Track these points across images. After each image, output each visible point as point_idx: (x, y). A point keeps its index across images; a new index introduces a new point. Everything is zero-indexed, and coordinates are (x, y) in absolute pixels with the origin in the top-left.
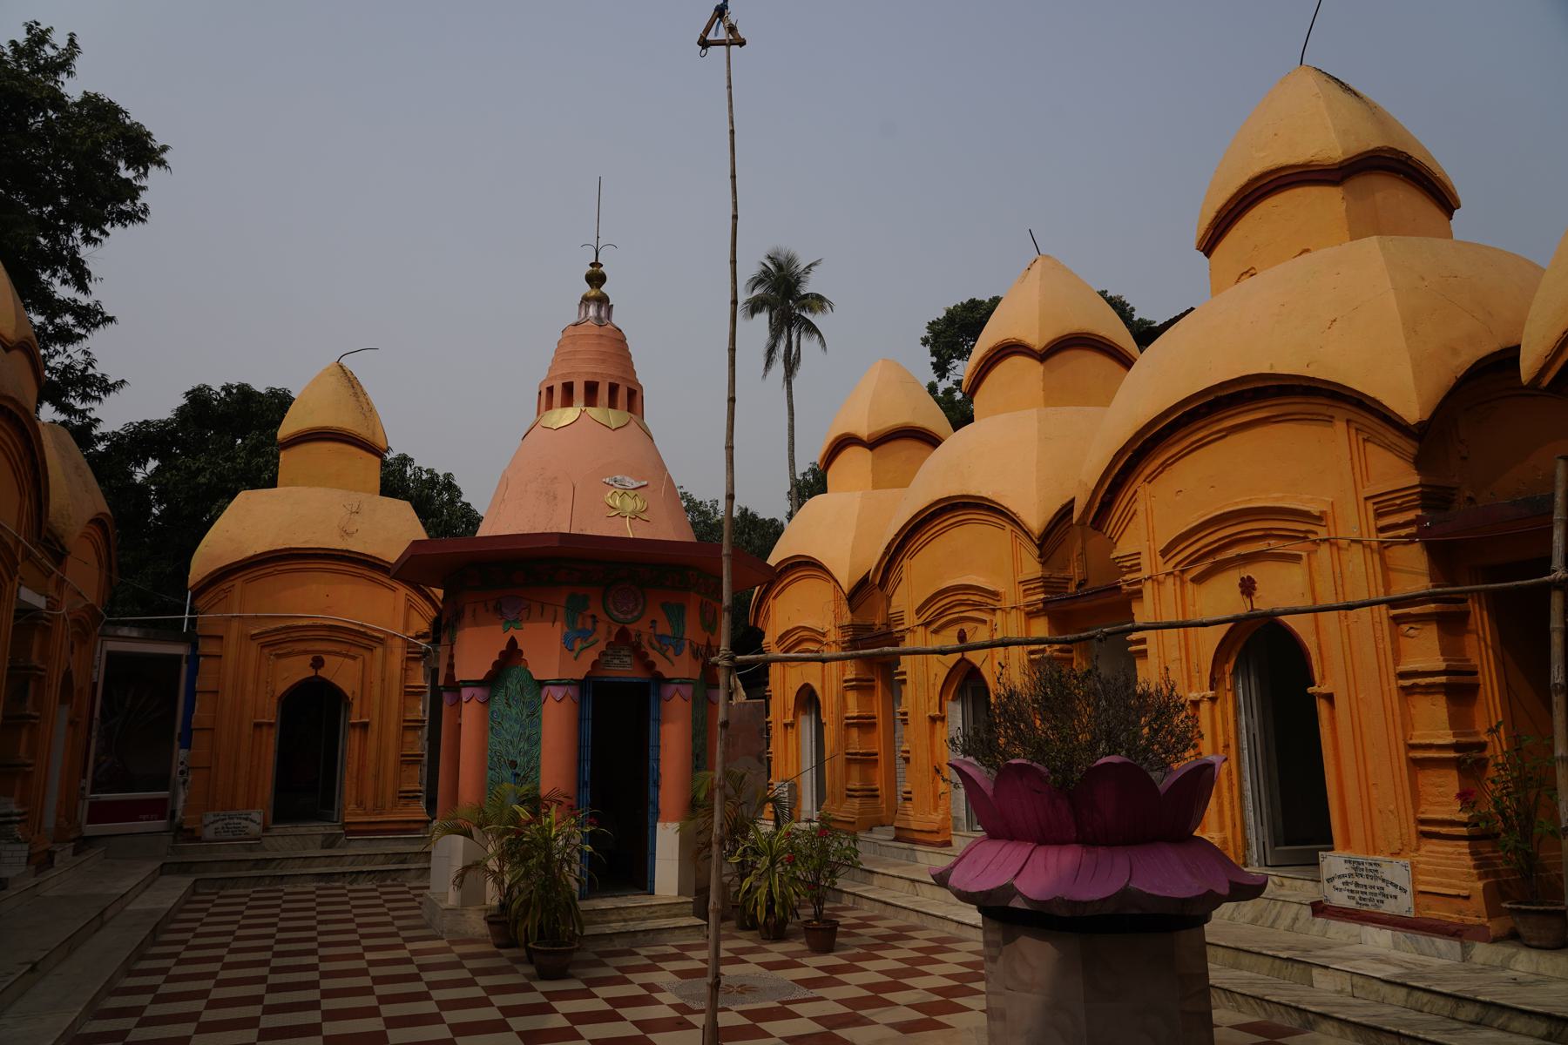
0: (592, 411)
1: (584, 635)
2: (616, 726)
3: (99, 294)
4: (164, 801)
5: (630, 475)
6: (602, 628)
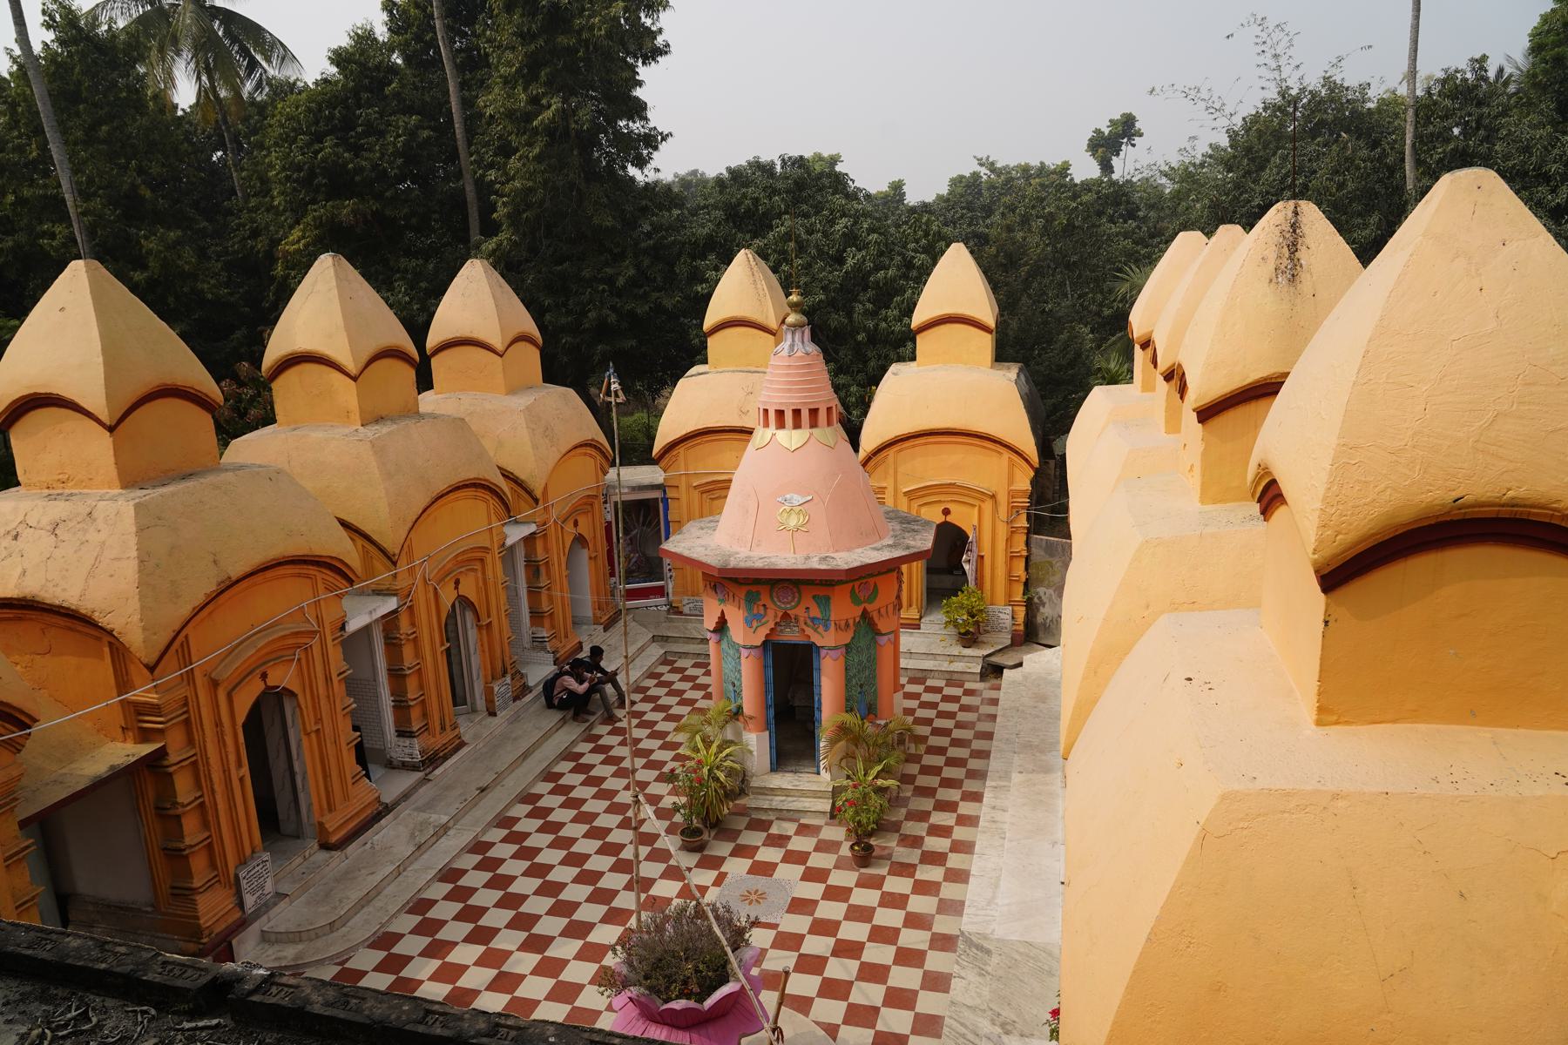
0: (781, 434)
1: (759, 617)
2: (790, 670)
3: (657, 119)
4: (662, 587)
5: (798, 493)
6: (771, 613)
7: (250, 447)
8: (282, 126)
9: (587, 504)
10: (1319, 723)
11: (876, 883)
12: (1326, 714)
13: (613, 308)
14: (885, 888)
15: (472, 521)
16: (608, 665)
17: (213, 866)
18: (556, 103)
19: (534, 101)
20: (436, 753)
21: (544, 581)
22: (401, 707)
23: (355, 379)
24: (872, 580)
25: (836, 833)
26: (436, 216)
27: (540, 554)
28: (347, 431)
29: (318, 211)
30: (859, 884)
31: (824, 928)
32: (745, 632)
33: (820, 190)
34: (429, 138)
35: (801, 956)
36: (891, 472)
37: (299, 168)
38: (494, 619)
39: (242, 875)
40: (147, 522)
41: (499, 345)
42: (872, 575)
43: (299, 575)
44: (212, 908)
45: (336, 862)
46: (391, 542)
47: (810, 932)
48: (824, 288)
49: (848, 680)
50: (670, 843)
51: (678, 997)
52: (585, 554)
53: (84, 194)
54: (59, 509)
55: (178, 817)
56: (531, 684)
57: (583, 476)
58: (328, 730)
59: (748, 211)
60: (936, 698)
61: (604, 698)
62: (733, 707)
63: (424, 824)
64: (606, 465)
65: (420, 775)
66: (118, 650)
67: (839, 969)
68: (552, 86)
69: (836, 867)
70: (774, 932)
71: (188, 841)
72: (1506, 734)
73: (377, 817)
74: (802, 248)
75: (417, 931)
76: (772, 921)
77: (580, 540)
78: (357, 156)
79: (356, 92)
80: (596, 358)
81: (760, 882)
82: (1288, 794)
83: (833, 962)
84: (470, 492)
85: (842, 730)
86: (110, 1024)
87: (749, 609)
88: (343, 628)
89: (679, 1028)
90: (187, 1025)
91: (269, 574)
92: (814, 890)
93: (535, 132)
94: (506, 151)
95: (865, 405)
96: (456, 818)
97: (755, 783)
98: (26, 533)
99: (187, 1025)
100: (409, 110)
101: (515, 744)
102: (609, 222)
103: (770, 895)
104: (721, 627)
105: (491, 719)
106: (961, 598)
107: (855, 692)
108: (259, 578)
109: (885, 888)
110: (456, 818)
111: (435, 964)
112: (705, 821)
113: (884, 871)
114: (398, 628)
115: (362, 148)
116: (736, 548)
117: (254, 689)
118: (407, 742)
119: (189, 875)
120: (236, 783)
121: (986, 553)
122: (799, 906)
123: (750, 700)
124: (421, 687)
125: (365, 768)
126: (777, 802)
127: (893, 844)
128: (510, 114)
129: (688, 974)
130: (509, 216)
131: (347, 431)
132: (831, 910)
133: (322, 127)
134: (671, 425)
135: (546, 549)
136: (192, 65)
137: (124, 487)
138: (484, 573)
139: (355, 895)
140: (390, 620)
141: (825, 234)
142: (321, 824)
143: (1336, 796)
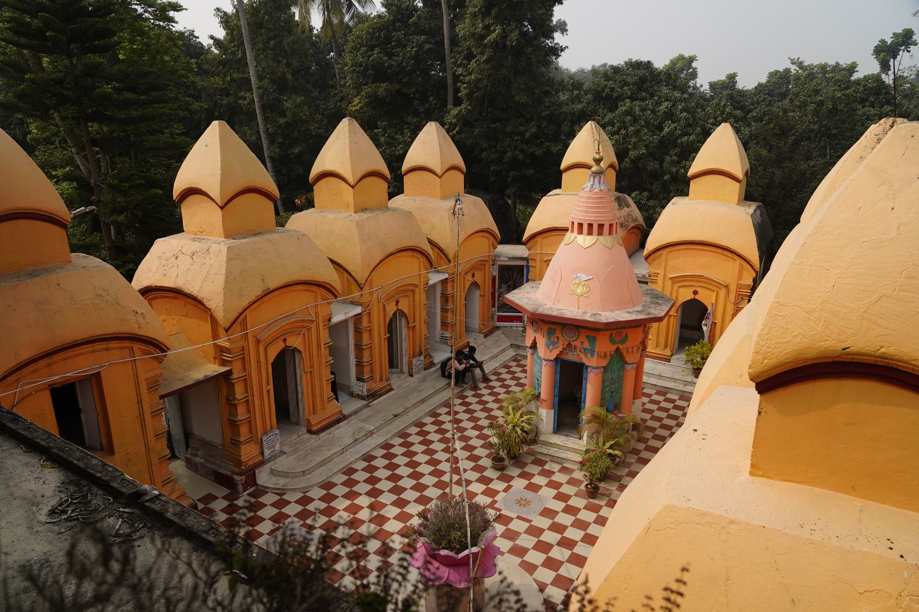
0: (580, 237)
2: (570, 378)
6: (561, 342)
7: (299, 221)
8: (353, 42)
9: (481, 265)
10: (751, 474)
11: (596, 509)
12: (756, 469)
13: (522, 151)
14: (600, 513)
15: (409, 270)
16: (478, 356)
17: (251, 432)
18: (498, 30)
19: (487, 27)
20: (376, 392)
21: (450, 306)
22: (360, 365)
23: (353, 187)
24: (624, 331)
25: (579, 475)
26: (429, 93)
27: (450, 291)
28: (346, 215)
29: (367, 89)
30: (586, 508)
31: (558, 528)
32: (546, 351)
33: (658, 83)
34: (430, 48)
35: (539, 541)
36: (663, 264)
37: (361, 65)
38: (417, 324)
39: (264, 439)
40: (233, 256)
41: (439, 171)
42: (625, 328)
43: (308, 290)
44: (248, 453)
45: (314, 440)
46: (361, 276)
47: (544, 530)
48: (646, 146)
49: (603, 388)
50: (486, 462)
51: (443, 548)
52: (477, 293)
53: (260, 78)
54: (196, 246)
55: (236, 405)
56: (436, 362)
57: (481, 248)
58: (316, 372)
59: (607, 95)
60: (670, 405)
61: (473, 376)
62: (537, 392)
63: (362, 428)
64: (495, 243)
65: (365, 402)
66: (213, 320)
67: (559, 553)
68: (499, 19)
69: (575, 495)
70: (527, 525)
71: (239, 418)
72: (873, 506)
73: (338, 421)
74: (635, 120)
75: (344, 484)
76: (530, 518)
77: (475, 285)
78: (390, 58)
79: (393, 22)
80: (510, 179)
81: (530, 495)
82: (704, 514)
83: (556, 548)
84: (409, 253)
85: (595, 418)
86: (95, 501)
87: (549, 338)
88: (330, 320)
89: (444, 565)
90: (121, 510)
91: (291, 288)
92: (559, 506)
93: (486, 45)
94: (469, 57)
95: (651, 222)
96: (378, 428)
97: (542, 438)
98: (181, 256)
99: (121, 510)
100: (422, 33)
101: (418, 393)
102: (524, 99)
103: (519, 507)
104: (534, 346)
105: (410, 378)
106: (697, 347)
107: (607, 396)
108: (286, 290)
109: (600, 513)
110: (378, 428)
111: (348, 503)
112: (508, 453)
113: (603, 503)
114: (361, 323)
115: (393, 54)
116: (546, 302)
117: (280, 346)
118: (361, 384)
119: (238, 434)
120: (265, 393)
121: (718, 321)
122: (548, 513)
123: (545, 390)
124: (371, 356)
125: (336, 394)
126: (552, 451)
127: (614, 488)
128: (473, 35)
129: (456, 538)
130: (467, 95)
131: (346, 215)
132: (565, 519)
133: (374, 42)
134: (535, 224)
135: (453, 288)
136: (321, 7)
137: (227, 237)
138: (414, 300)
139: (319, 459)
140: (358, 317)
141: (653, 112)
142: (308, 420)
143: (732, 522)
